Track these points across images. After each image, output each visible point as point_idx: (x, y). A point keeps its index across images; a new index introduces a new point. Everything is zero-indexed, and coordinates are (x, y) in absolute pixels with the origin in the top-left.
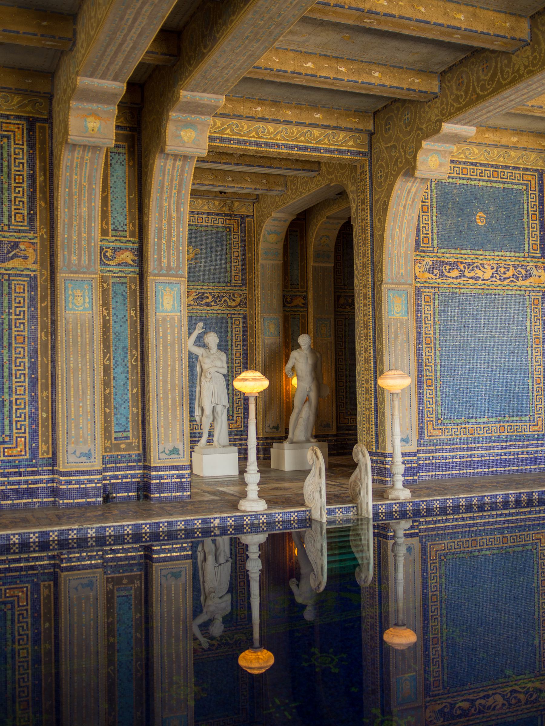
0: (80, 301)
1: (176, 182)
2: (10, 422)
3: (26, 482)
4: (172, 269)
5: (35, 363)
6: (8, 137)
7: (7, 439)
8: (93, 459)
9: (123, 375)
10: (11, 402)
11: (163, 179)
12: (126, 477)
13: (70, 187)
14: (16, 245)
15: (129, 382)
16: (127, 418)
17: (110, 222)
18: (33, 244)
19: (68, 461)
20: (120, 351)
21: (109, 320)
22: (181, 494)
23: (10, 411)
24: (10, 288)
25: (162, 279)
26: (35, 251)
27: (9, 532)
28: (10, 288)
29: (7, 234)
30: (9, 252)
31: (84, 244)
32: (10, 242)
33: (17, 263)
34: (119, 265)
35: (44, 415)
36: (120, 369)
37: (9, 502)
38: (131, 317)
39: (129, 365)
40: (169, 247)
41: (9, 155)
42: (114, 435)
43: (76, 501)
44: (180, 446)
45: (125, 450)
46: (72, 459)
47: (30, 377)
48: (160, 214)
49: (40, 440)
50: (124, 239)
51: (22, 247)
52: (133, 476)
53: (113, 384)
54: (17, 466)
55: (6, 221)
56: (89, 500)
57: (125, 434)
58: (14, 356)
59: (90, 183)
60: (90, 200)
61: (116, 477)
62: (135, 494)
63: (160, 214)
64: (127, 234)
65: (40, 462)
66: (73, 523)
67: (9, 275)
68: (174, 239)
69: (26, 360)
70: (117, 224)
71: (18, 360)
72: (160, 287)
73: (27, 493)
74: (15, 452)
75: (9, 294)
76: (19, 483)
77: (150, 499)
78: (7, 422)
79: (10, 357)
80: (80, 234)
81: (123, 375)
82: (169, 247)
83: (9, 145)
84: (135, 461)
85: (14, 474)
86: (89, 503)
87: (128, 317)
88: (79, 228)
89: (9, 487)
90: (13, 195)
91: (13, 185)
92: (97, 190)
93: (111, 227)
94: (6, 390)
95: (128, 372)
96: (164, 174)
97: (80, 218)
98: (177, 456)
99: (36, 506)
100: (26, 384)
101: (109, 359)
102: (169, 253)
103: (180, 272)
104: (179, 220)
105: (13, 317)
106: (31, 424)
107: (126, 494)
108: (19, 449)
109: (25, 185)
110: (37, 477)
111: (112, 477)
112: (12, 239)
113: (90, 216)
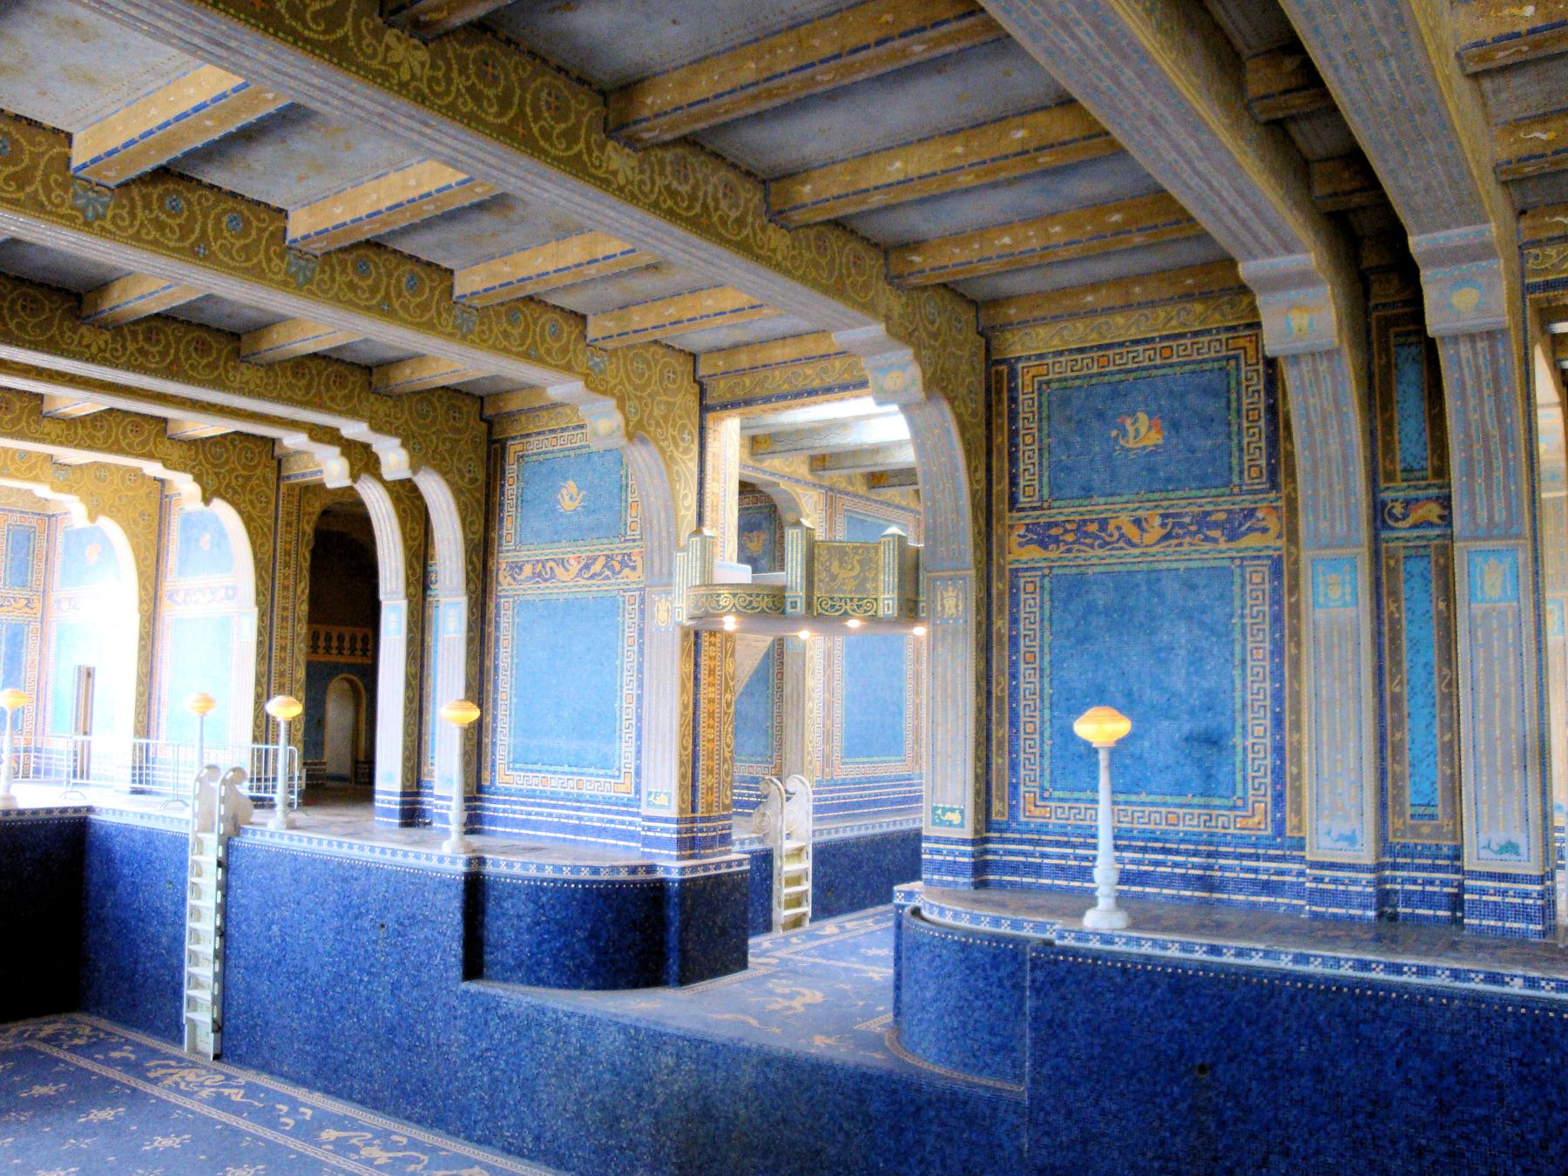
0: (1335, 593)
1: (1487, 376)
2: (1245, 779)
3: (1267, 870)
4: (1496, 526)
5: (1282, 688)
6: (1236, 358)
7: (1240, 803)
8: (1358, 847)
9: (1426, 711)
10: (1245, 749)
11: (1462, 374)
12: (1431, 883)
13: (1307, 416)
14: (1251, 513)
15: (1437, 722)
16: (1433, 783)
17: (1398, 457)
18: (1275, 508)
19: (1321, 847)
20: (1419, 669)
21: (1399, 620)
22: (1523, 926)
23: (1244, 762)
24: (1243, 577)
25: (1480, 545)
26: (1279, 518)
27: (1166, 937)
28: (1243, 577)
29: (1238, 499)
30: (1241, 525)
31: (1339, 501)
32: (1242, 510)
33: (1252, 541)
34: (1415, 526)
35: (1295, 770)
36: (1420, 699)
37: (1241, 897)
38: (1439, 612)
39: (1436, 692)
40: (1489, 487)
41: (1239, 383)
42: (1409, 811)
43: (1331, 910)
44: (1520, 839)
45: (1429, 836)
46: (1326, 842)
47: (1274, 713)
48: (1468, 436)
49: (1288, 809)
50: (1423, 483)
51: (1260, 515)
52: (1444, 883)
53: (1407, 724)
54: (1255, 846)
55: (1236, 480)
56: (1352, 912)
57: (1429, 811)
58: (1250, 679)
59: (1337, 405)
60: (1341, 432)
61: (1414, 882)
62: (1448, 913)
63: (1468, 436)
64: (1429, 472)
65: (1288, 843)
66: (1259, 940)
67: (1242, 558)
68: (1498, 474)
69: (1267, 684)
70: (1410, 459)
71: (1256, 686)
72: (1479, 560)
73: (1268, 887)
74: (1251, 822)
75: (1243, 586)
76: (1256, 871)
77: (1463, 926)
78: (1239, 777)
79: (1244, 679)
80: (1330, 485)
81: (1426, 711)
82: (1489, 487)
83: (1238, 369)
84: (1448, 857)
85: (1249, 856)
86: (1352, 917)
87: (1433, 612)
88: (1330, 477)
89: (1242, 875)
90: (1245, 441)
91: (1245, 424)
92: (1351, 414)
93: (1399, 467)
94: (1238, 730)
95: (1434, 705)
96: (1461, 368)
97: (1330, 462)
98: (1514, 857)
99: (1282, 909)
100: (1268, 722)
101: (1401, 683)
102: (1489, 498)
103: (1514, 530)
104: (1504, 440)
105: (1248, 621)
106: (1275, 783)
107: (1431, 912)
108: (1256, 820)
109: (1262, 423)
110: (1284, 866)
111: (1404, 881)
112: (1246, 505)
113: (1345, 458)
